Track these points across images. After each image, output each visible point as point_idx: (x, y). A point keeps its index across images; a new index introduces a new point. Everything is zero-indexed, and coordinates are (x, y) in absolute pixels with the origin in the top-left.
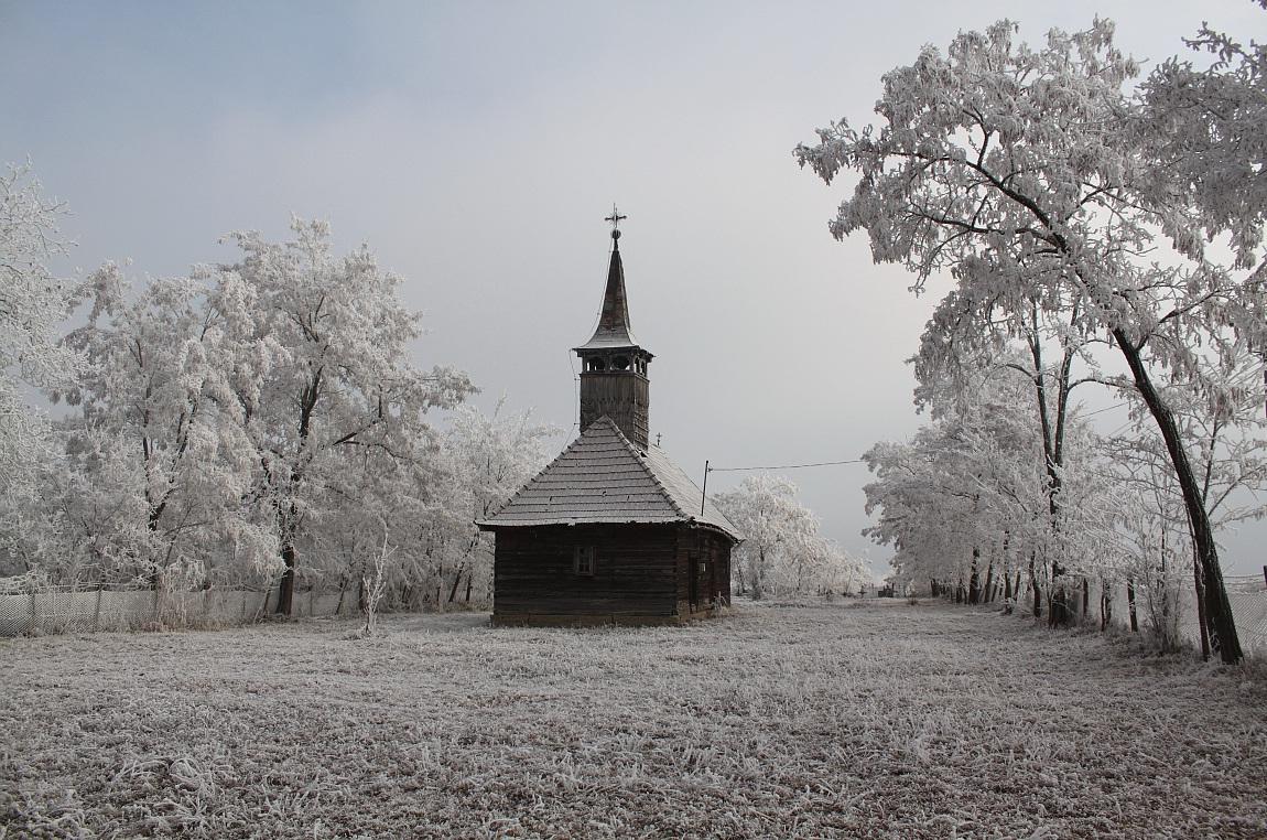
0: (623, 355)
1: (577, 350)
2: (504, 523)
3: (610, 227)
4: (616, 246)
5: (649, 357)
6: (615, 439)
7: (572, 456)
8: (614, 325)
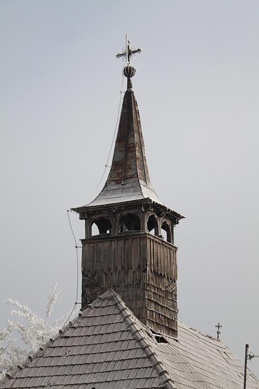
0: (133, 212)
1: (77, 210)
3: (123, 63)
4: (129, 85)
5: (175, 218)
6: (118, 318)
7: (62, 342)
8: (126, 178)
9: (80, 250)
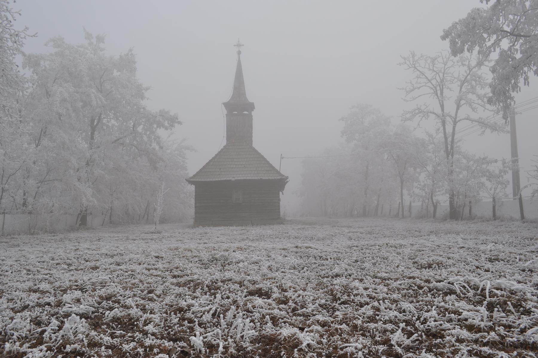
2: (197, 180)
9: (225, 118)
